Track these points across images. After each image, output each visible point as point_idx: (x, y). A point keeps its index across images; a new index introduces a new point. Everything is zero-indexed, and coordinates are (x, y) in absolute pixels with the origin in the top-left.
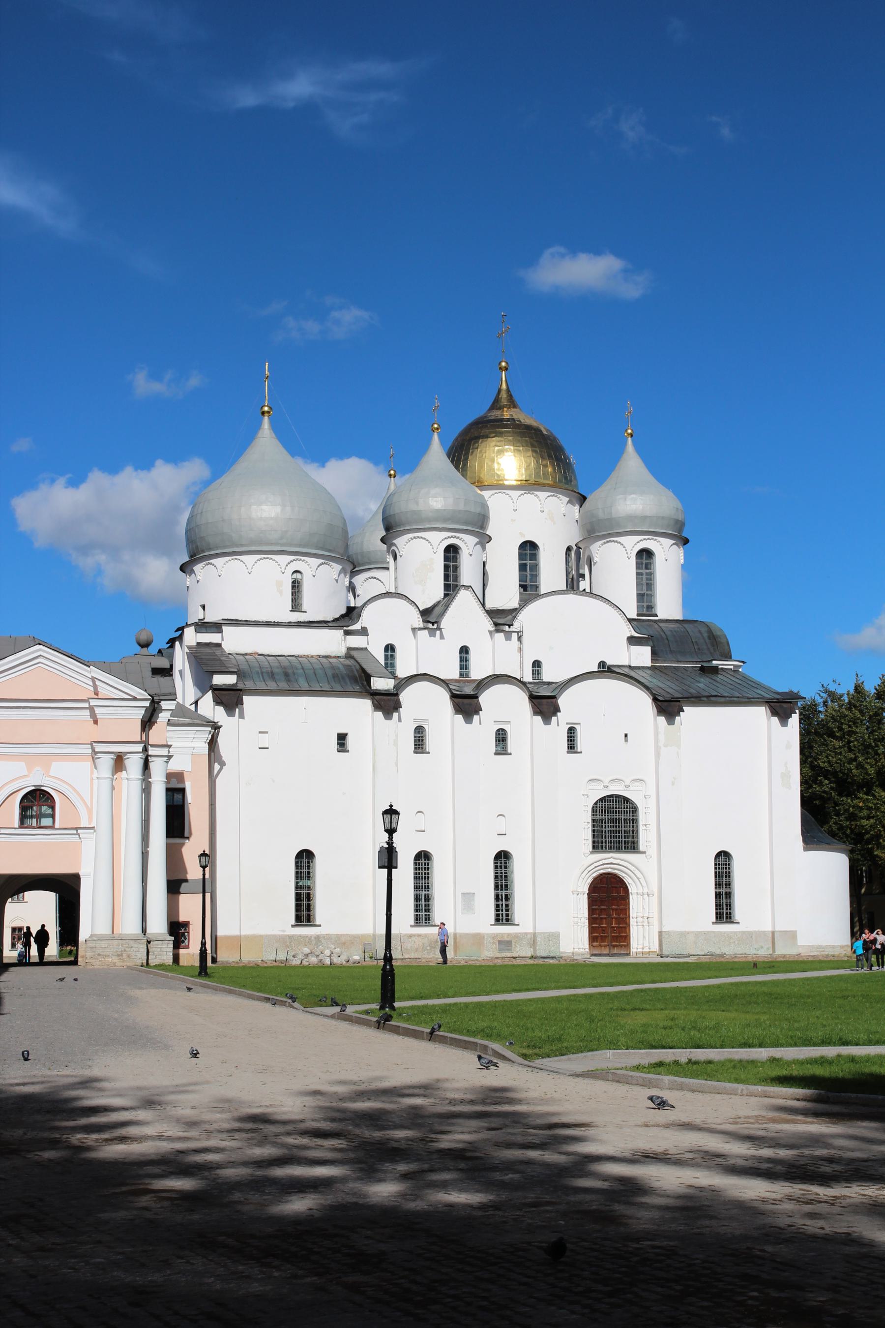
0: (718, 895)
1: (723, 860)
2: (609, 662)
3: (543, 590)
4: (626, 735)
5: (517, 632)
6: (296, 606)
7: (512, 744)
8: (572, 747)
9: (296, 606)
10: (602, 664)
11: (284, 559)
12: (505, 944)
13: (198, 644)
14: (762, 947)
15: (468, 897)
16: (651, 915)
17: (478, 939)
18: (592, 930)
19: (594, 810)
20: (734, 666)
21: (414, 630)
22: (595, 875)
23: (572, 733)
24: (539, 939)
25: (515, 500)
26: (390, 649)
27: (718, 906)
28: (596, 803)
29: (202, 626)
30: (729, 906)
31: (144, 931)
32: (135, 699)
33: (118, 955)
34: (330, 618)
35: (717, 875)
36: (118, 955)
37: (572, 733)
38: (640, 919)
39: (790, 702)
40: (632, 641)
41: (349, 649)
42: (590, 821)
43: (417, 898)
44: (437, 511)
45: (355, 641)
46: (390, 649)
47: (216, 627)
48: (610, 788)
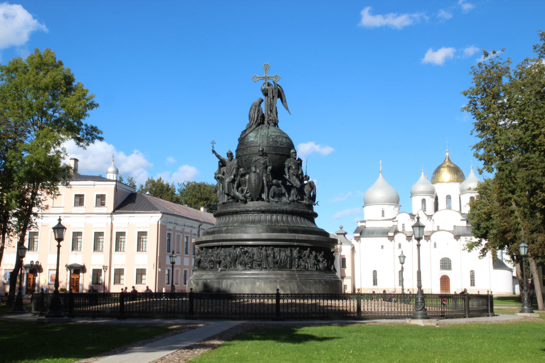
0: (471, 280)
2: (456, 225)
3: (439, 209)
6: (383, 216)
8: (435, 246)
9: (383, 216)
10: (455, 226)
18: (441, 288)
19: (441, 261)
21: (409, 220)
23: (435, 244)
26: (403, 225)
27: (471, 283)
29: (362, 222)
30: (474, 283)
34: (392, 218)
37: (435, 244)
45: (395, 223)
46: (403, 225)
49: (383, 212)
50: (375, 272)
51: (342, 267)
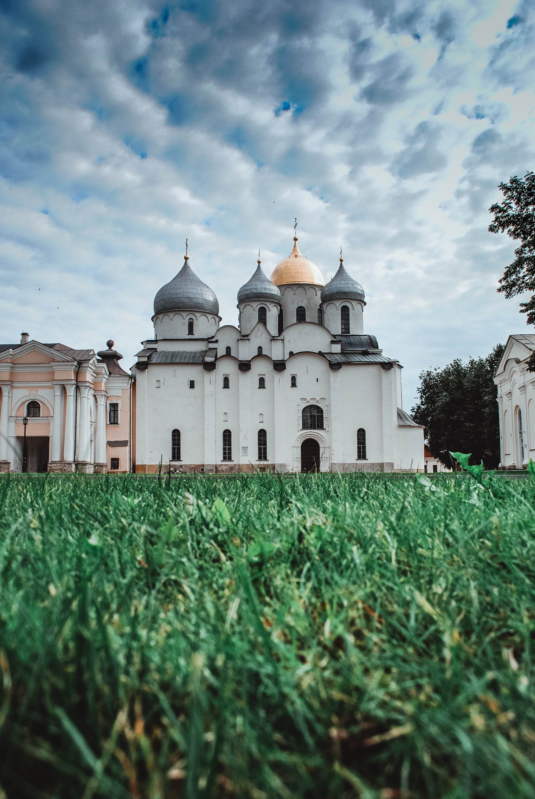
1: (361, 433)
4: (317, 379)
5: (282, 340)
6: (191, 332)
7: (267, 384)
8: (294, 385)
9: (191, 332)
11: (184, 314)
12: (263, 469)
13: (148, 349)
14: (378, 470)
15: (245, 448)
16: (328, 456)
17: (251, 467)
19: (304, 411)
20: (378, 352)
21: (238, 340)
22: (304, 439)
23: (294, 379)
24: (276, 466)
25: (295, 290)
26: (228, 349)
27: (359, 452)
28: (304, 408)
30: (364, 452)
31: (74, 460)
32: (68, 361)
33: (60, 470)
34: (206, 337)
35: (359, 439)
36: (60, 470)
37: (294, 379)
38: (324, 458)
39: (392, 363)
40: (333, 342)
41: (210, 349)
42: (301, 416)
43: (224, 449)
44: (255, 293)
45: (211, 346)
46: (228, 349)
47: (156, 341)
48: (310, 402)
49: (191, 326)
50: (176, 434)
51: (111, 423)
